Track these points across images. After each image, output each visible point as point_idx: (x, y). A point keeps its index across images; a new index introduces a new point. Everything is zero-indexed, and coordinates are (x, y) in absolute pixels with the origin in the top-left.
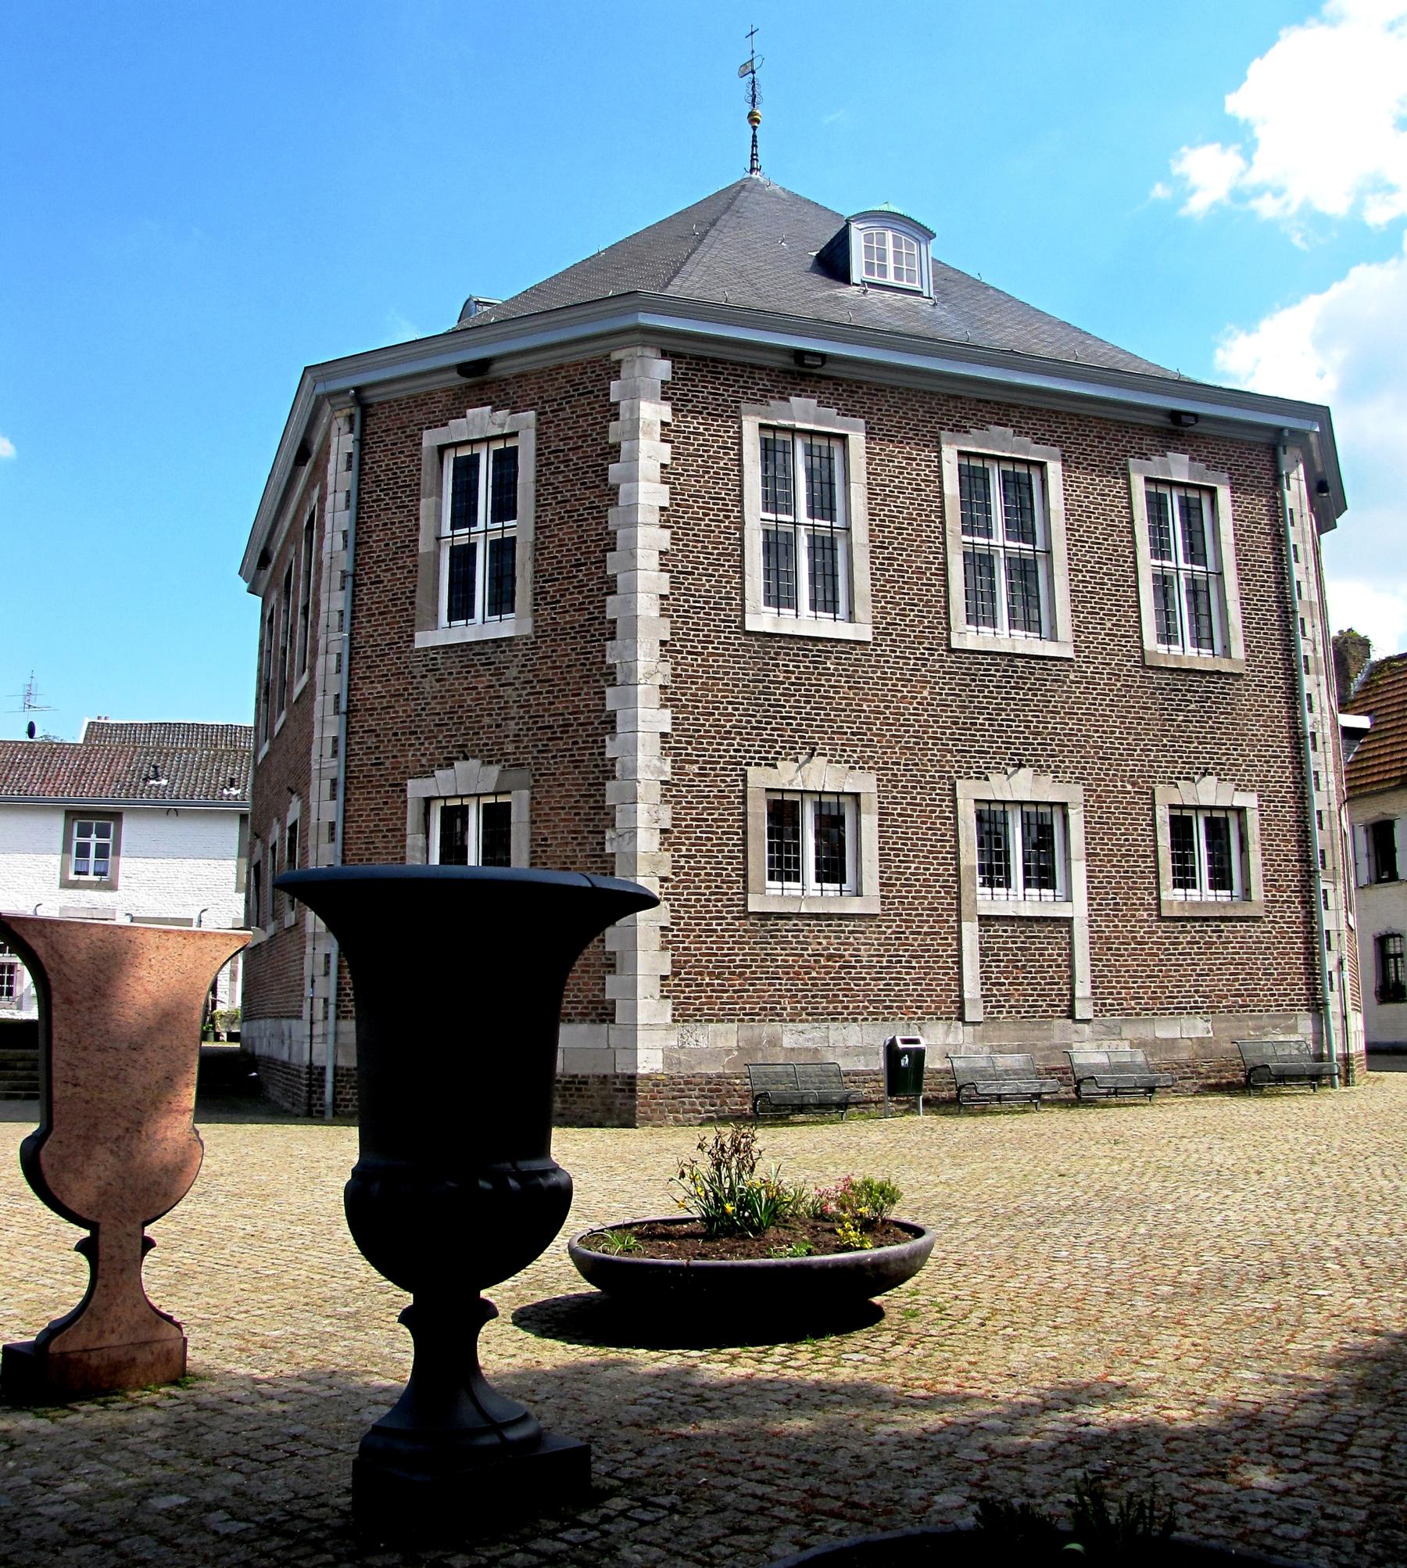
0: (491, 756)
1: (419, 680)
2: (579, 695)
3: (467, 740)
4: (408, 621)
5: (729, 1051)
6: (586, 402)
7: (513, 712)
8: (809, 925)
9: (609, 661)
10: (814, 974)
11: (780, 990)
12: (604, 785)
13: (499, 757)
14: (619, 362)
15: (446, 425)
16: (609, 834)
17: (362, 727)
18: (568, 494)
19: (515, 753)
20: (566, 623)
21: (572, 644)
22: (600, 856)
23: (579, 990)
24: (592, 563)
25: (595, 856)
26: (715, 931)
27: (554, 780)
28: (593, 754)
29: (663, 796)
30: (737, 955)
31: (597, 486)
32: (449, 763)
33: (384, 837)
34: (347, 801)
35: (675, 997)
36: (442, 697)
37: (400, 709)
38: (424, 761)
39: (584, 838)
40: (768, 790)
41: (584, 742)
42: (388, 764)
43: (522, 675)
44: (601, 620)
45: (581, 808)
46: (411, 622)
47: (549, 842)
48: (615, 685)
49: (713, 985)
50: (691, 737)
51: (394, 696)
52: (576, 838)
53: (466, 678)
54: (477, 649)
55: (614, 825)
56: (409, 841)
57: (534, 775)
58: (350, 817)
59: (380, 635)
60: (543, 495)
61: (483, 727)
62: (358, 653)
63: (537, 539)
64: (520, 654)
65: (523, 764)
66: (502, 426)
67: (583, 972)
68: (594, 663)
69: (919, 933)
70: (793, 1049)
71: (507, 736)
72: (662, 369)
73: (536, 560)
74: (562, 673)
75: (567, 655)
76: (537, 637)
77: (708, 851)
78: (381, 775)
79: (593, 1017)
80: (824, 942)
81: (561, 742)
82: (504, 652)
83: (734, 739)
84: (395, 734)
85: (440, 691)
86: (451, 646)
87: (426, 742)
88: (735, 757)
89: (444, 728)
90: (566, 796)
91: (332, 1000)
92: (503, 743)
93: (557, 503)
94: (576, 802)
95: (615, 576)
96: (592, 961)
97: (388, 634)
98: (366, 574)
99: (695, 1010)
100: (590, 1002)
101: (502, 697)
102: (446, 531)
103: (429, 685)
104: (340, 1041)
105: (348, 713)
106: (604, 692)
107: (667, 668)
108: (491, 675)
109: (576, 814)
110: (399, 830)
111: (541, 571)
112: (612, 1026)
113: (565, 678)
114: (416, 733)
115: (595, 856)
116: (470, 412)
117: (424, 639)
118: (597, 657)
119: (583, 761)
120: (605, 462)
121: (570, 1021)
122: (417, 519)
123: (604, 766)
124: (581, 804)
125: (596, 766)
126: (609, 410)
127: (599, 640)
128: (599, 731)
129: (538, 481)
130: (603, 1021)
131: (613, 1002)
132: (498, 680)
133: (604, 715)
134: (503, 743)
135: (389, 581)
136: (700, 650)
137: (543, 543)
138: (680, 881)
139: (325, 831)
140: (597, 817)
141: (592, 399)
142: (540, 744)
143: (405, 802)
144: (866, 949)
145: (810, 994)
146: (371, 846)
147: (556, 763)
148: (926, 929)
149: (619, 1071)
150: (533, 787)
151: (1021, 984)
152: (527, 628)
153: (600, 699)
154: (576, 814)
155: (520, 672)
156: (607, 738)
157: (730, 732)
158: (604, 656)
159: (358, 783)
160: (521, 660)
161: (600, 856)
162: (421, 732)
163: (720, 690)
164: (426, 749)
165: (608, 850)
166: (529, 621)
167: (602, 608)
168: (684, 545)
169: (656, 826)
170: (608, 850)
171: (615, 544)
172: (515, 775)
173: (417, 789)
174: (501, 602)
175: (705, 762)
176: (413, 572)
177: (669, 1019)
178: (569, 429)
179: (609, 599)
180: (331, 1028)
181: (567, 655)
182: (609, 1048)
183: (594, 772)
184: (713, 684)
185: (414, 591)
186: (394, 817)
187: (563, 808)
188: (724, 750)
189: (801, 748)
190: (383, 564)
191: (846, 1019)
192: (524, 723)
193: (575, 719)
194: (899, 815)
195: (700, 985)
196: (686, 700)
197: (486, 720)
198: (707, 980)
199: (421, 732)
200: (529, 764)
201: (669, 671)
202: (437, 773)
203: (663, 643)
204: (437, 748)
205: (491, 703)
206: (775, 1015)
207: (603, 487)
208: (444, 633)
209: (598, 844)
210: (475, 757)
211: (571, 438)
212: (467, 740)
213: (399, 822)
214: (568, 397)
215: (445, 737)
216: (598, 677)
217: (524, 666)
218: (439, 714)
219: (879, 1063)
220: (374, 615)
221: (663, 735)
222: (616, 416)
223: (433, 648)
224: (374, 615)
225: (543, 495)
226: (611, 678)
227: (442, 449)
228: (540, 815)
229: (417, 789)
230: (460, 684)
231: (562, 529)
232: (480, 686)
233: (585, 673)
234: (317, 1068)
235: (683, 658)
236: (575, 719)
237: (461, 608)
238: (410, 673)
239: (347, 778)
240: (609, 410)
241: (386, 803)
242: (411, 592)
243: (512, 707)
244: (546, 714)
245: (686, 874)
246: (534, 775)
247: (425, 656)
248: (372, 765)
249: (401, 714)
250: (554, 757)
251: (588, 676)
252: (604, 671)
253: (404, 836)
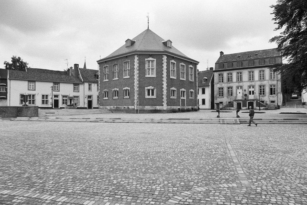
32: (149, 86)
117: (146, 76)
173: (146, 88)
206: (171, 106)
222: (163, 61)
229: (146, 88)
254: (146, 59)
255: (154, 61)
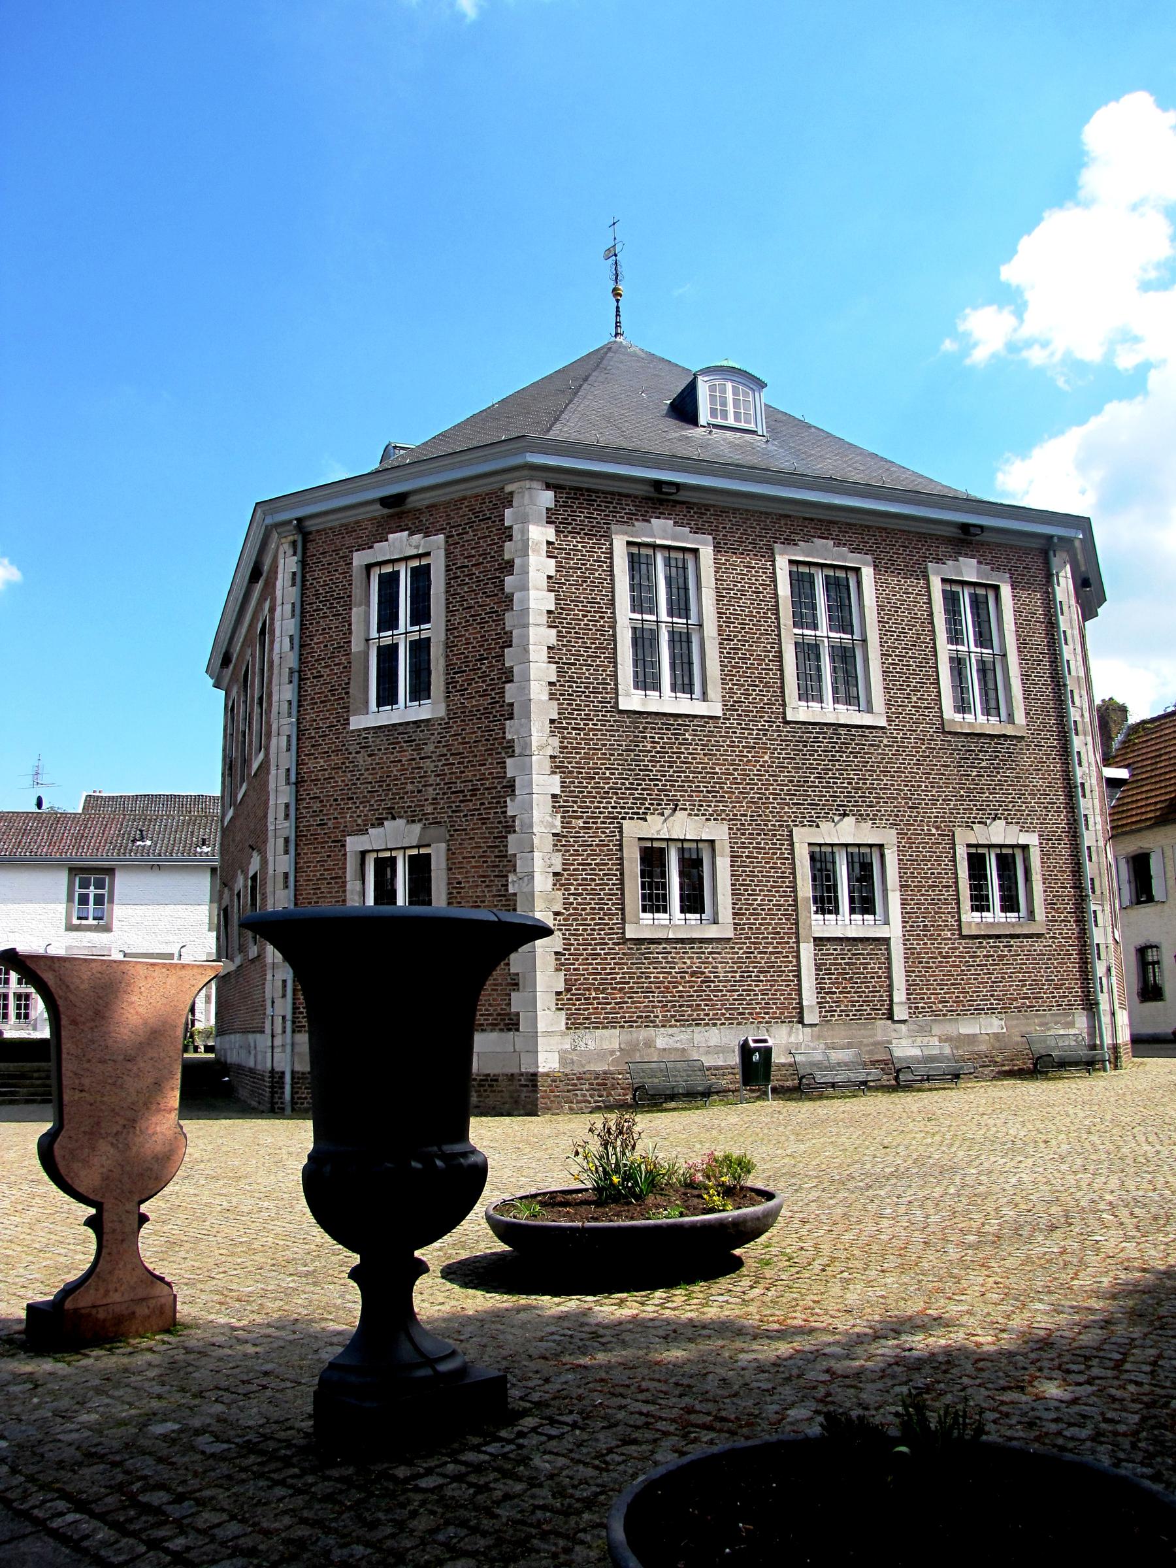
0: (414, 816)
1: (354, 755)
2: (485, 765)
3: (394, 803)
4: (344, 708)
5: (612, 1052)
6: (485, 526)
7: (431, 780)
8: (676, 948)
9: (509, 736)
10: (680, 988)
11: (653, 1002)
12: (506, 837)
13: (420, 817)
14: (511, 493)
15: (371, 547)
16: (511, 877)
17: (309, 794)
18: (472, 602)
19: (433, 813)
20: (473, 706)
21: (478, 723)
22: (504, 896)
23: (490, 1005)
24: (493, 657)
25: (500, 896)
26: (599, 954)
27: (466, 834)
28: (497, 813)
29: (555, 845)
30: (618, 974)
31: (496, 595)
33: (328, 884)
34: (297, 855)
35: (568, 1009)
36: (373, 769)
37: (340, 780)
38: (359, 821)
39: (492, 881)
40: (640, 839)
41: (489, 803)
42: (330, 825)
43: (438, 750)
44: (501, 703)
45: (489, 857)
46: (347, 708)
47: (463, 885)
48: (513, 756)
49: (598, 998)
50: (576, 797)
51: (334, 769)
52: (484, 882)
53: (393, 753)
54: (401, 729)
55: (515, 870)
56: (349, 887)
57: (449, 831)
58: (300, 868)
59: (321, 719)
60: (452, 603)
61: (407, 793)
62: (304, 735)
63: (448, 639)
64: (436, 732)
65: (440, 822)
66: (417, 547)
67: (492, 990)
68: (496, 739)
69: (765, 953)
70: (664, 1049)
71: (426, 800)
72: (547, 498)
73: (447, 656)
74: (470, 747)
75: (475, 733)
76: (449, 719)
77: (592, 889)
78: (325, 834)
79: (502, 1026)
80: (688, 961)
81: (471, 804)
82: (423, 731)
83: (611, 798)
84: (336, 800)
85: (372, 764)
86: (380, 727)
87: (361, 806)
88: (613, 813)
89: (375, 794)
90: (476, 847)
91: (289, 1017)
92: (423, 805)
93: (463, 609)
94: (484, 852)
95: (512, 667)
96: (500, 981)
97: (328, 718)
98: (309, 670)
99: (584, 1019)
100: (499, 1014)
101: (422, 768)
102: (374, 634)
103: (362, 759)
104: (296, 1051)
105: (297, 783)
106: (505, 762)
107: (555, 742)
108: (412, 750)
109: (484, 862)
110: (341, 877)
111: (452, 665)
112: (517, 1033)
113: (473, 752)
114: (352, 798)
115: (500, 896)
116: (391, 536)
117: (357, 722)
118: (498, 734)
119: (489, 818)
120: (502, 575)
121: (482, 1030)
122: (350, 625)
123: (506, 822)
124: (488, 854)
125: (500, 822)
126: (504, 533)
127: (500, 720)
128: (502, 794)
129: (447, 592)
130: (510, 1030)
131: (518, 1014)
132: (419, 754)
133: (505, 781)
134: (423, 805)
135: (328, 675)
136: (582, 726)
137: (453, 642)
138: (570, 915)
139: (280, 880)
140: (501, 864)
141: (490, 524)
142: (453, 805)
143: (345, 855)
144: (722, 966)
145: (677, 1004)
146: (318, 891)
147: (467, 821)
148: (770, 950)
149: (523, 1070)
150: (449, 840)
151: (849, 992)
152: (442, 712)
153: (501, 768)
154: (484, 862)
155: (436, 747)
156: (508, 799)
157: (608, 793)
158: (504, 733)
159: (306, 840)
160: (436, 737)
161: (504, 896)
162: (357, 798)
163: (599, 759)
164: (361, 811)
165: (511, 891)
166: (443, 705)
167: (502, 694)
168: (568, 641)
169: (550, 870)
170: (511, 891)
171: (511, 641)
172: (434, 831)
173: (354, 844)
174: (420, 690)
175: (588, 817)
176: (347, 668)
177: (563, 1027)
178: (472, 548)
179: (508, 686)
180: (289, 1041)
181: (475, 733)
182: (515, 1051)
183: (498, 828)
184: (593, 754)
185: (348, 683)
186: (336, 867)
187: (474, 857)
188: (604, 808)
189: (666, 804)
190: (323, 662)
191: (707, 1024)
192: (440, 789)
193: (482, 784)
194: (747, 857)
195: (589, 999)
196: (572, 767)
197: (409, 787)
198: (594, 995)
199: (357, 798)
200: (445, 822)
201: (557, 744)
202: (370, 831)
203: (552, 721)
204: (370, 810)
205: (413, 773)
206: (649, 1022)
207: (500, 595)
208: (373, 717)
209: (502, 885)
210: (401, 817)
211: (473, 556)
212: (394, 803)
213: (340, 872)
214: (470, 523)
215: (376, 801)
216: (500, 750)
217: (439, 742)
218: (371, 783)
219: (735, 1059)
220: (316, 703)
221: (554, 796)
222: (510, 538)
223: (365, 729)
224: (316, 703)
225: (452, 603)
226: (510, 750)
227: (369, 567)
228: (455, 863)
229: (354, 844)
230: (387, 758)
231: (468, 630)
232: (404, 759)
233: (489, 747)
234: (277, 1073)
235: (568, 733)
236: (482, 784)
237: (387, 696)
238: (347, 749)
239: (297, 836)
240: (504, 533)
241: (329, 856)
242: (346, 684)
243: (430, 776)
244: (458, 781)
245: (575, 909)
246: (449, 831)
247: (359, 735)
248: (317, 825)
249: (340, 783)
250: (465, 816)
251: (491, 749)
252: (505, 745)
253: (345, 882)
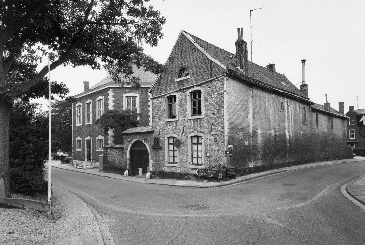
254: (125, 95)
255: (136, 97)
